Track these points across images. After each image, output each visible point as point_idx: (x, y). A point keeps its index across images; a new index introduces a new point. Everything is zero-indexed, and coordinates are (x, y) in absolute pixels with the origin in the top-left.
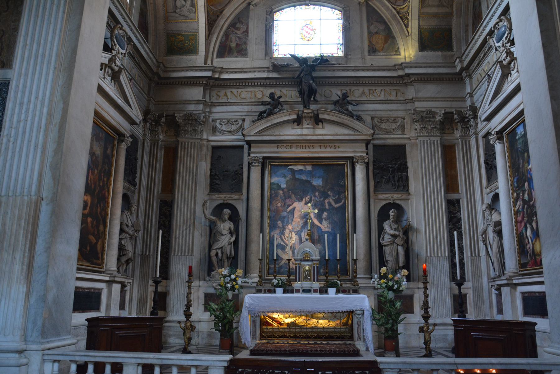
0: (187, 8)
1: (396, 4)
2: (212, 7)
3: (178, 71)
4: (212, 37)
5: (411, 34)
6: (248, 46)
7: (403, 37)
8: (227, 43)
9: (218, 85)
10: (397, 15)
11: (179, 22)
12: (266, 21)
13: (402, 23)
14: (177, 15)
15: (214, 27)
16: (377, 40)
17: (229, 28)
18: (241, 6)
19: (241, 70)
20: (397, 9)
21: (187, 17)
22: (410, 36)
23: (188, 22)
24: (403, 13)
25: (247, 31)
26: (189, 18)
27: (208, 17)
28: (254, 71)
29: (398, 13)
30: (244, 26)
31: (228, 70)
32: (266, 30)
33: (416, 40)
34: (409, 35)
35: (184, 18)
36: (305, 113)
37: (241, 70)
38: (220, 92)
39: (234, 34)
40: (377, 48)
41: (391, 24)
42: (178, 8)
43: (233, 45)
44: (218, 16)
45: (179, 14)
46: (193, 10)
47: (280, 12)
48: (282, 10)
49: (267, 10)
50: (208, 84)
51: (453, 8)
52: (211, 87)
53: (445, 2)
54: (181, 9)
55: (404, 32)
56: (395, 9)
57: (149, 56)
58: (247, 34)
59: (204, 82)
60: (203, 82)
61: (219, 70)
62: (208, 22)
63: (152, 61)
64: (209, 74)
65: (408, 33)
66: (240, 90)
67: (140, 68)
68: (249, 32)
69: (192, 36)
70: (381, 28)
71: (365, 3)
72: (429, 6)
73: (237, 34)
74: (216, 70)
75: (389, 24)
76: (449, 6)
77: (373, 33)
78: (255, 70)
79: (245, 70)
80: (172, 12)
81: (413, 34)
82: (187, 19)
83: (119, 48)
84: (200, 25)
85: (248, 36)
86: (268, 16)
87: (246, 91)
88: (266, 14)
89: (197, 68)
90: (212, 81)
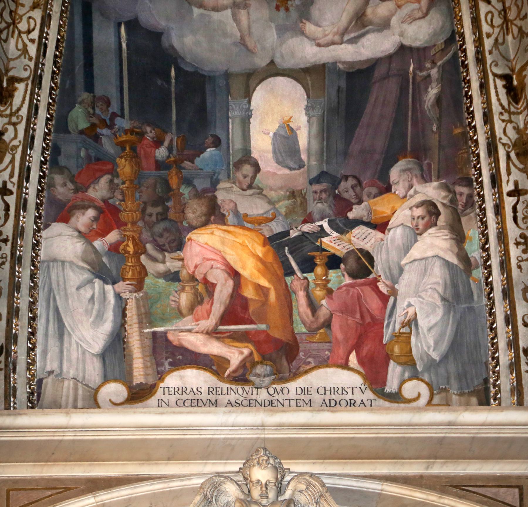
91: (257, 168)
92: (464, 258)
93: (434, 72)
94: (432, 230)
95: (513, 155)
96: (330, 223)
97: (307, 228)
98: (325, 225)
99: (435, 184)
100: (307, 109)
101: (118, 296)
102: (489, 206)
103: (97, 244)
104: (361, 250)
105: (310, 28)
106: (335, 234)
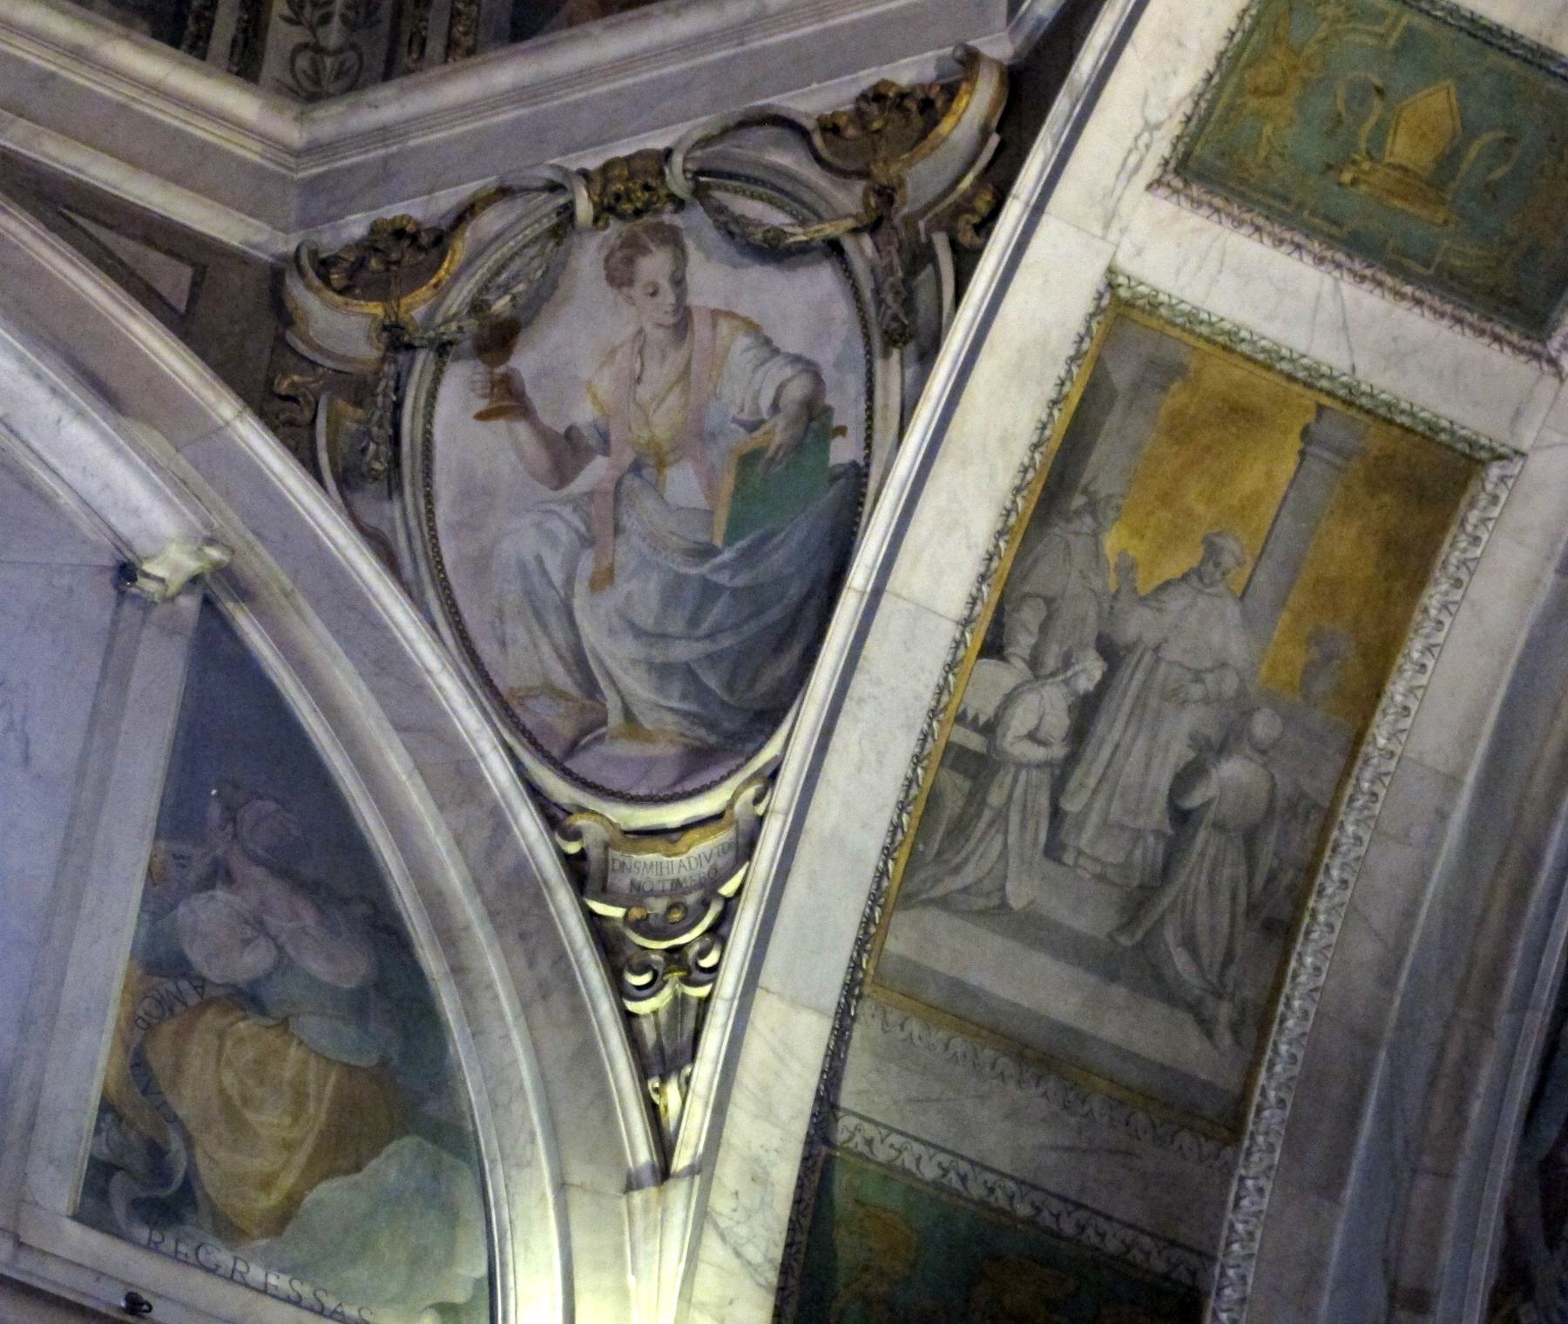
1: (583, 764)
5: (703, 1167)
7: (579, 1173)
10: (563, 898)
13: (605, 1007)
16: (228, 1079)
20: (580, 821)
22: (679, 1196)
24: (636, 895)
29: (578, 871)
33: (754, 1253)
34: (663, 1172)
40: (210, 1179)
41: (458, 971)
51: (1260, 1049)
53: (1189, 942)
55: (608, 1117)
56: (554, 818)
65: (664, 1144)
70: (316, 965)
71: (189, 604)
72: (997, 914)
75: (431, 961)
76: (1224, 1012)
77: (201, 983)
81: (729, 1172)
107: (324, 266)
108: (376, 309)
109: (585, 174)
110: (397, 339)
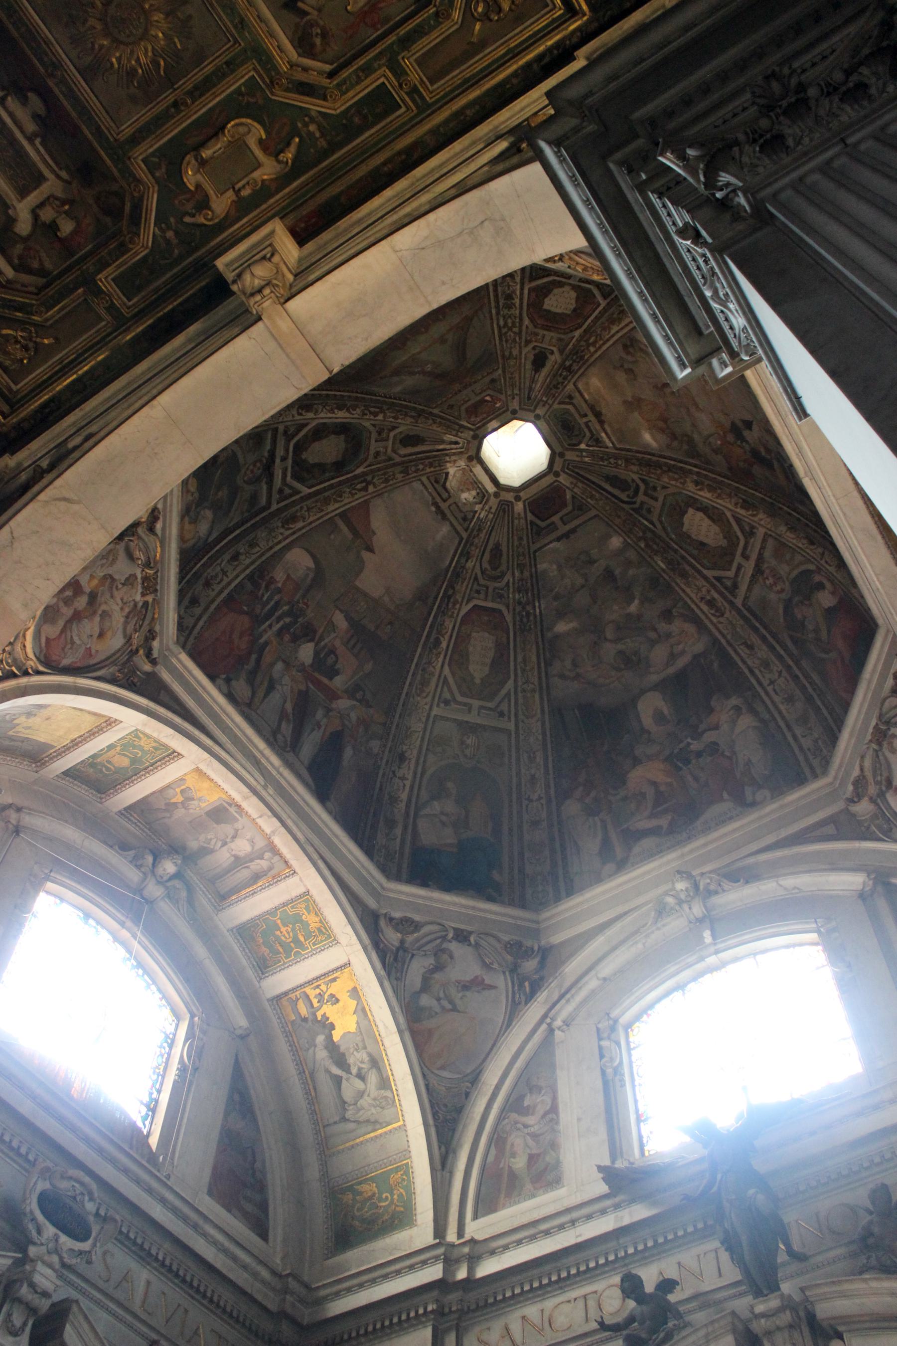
0: (372, 1096)
2: (445, 1074)
3: (349, 1290)
4: (455, 1158)
6: (562, 1151)
8: (501, 1166)
9: (478, 1305)
11: (357, 1144)
12: (602, 1056)
14: (351, 1126)
15: (461, 1127)
17: (504, 1119)
18: (530, 1046)
19: (531, 1231)
21: (376, 1122)
23: (381, 1135)
25: (554, 1109)
26: (381, 1124)
27: (430, 1101)
28: (573, 1222)
30: (544, 1098)
31: (494, 1244)
32: (606, 1084)
35: (370, 1128)
36: (763, 1315)
37: (531, 1231)
38: (489, 1329)
39: (519, 1129)
42: (350, 1105)
43: (520, 1163)
44: (467, 1095)
45: (354, 1122)
46: (386, 1098)
47: (645, 1017)
48: (649, 1012)
49: (600, 1026)
50: (447, 1310)
52: (459, 1319)
54: (355, 1104)
57: (234, 1259)
58: (554, 1116)
59: (430, 1308)
60: (425, 1309)
61: (466, 1250)
62: (435, 1119)
63: (255, 1275)
64: (434, 1273)
66: (549, 1304)
67: (213, 1304)
68: (561, 1107)
69: (397, 1172)
73: (526, 1126)
74: (456, 1253)
78: (575, 1215)
79: (544, 1227)
80: (335, 1123)
82: (378, 1126)
83: (56, 1239)
84: (410, 1133)
85: (557, 1123)
86: (604, 1043)
87: (569, 1301)
88: (600, 1039)
89: (398, 1266)
90: (453, 1297)
91: (649, 732)
92: (762, 721)
93: (713, 657)
94: (742, 717)
95: (762, 669)
96: (693, 739)
97: (681, 746)
98: (689, 740)
99: (734, 697)
100: (664, 699)
101: (602, 821)
102: (763, 694)
103: (587, 801)
104: (711, 743)
105: (652, 670)
106: (695, 742)
107: (851, 801)
108: (866, 798)
109: (871, 741)
110: (872, 800)
